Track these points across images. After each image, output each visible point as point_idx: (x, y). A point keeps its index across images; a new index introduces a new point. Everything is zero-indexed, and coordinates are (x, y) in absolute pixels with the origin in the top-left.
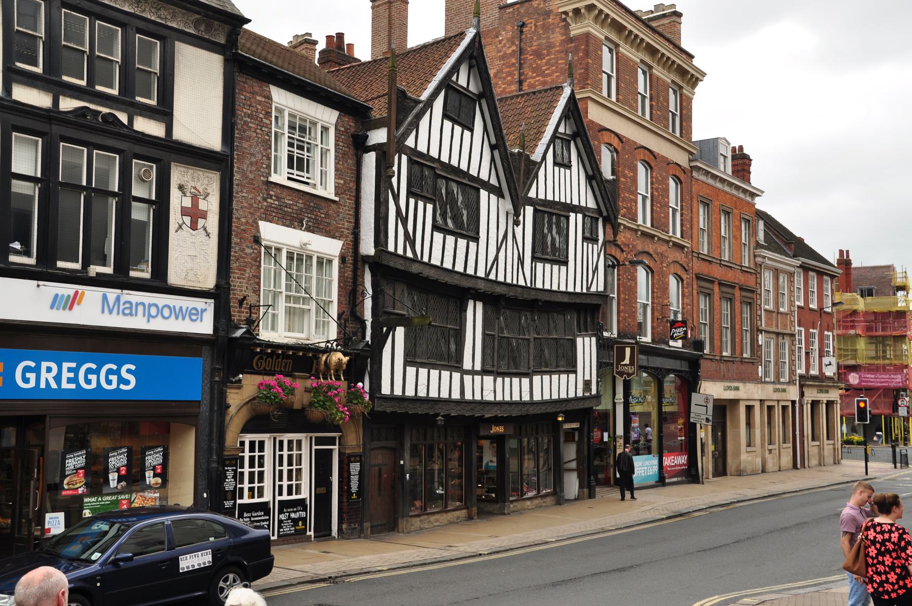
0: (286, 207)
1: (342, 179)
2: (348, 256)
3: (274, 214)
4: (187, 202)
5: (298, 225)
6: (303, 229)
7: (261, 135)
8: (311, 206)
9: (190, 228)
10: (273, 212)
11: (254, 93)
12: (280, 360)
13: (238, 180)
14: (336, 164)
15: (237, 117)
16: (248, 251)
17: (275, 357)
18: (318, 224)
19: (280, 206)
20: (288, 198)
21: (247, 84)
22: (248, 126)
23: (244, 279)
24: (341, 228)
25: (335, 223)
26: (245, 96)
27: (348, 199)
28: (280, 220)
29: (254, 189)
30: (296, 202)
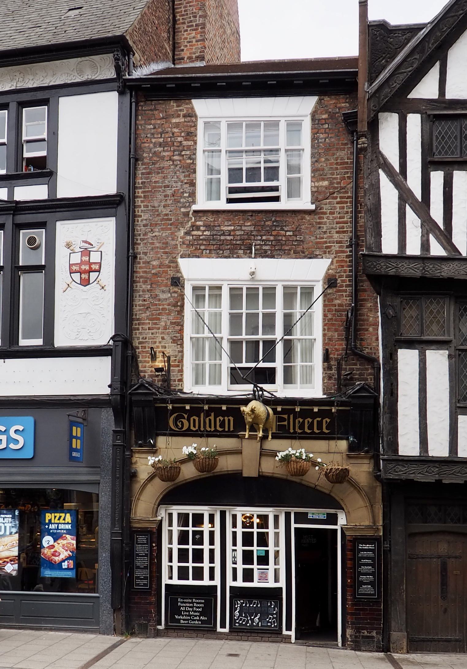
0: (223, 234)
1: (323, 180)
2: (341, 276)
3: (202, 247)
4: (76, 258)
5: (245, 253)
6: (253, 255)
7: (180, 161)
8: (268, 225)
9: (80, 284)
10: (202, 244)
11: (167, 118)
12: (212, 417)
13: (146, 220)
14: (313, 164)
15: (144, 151)
16: (162, 296)
17: (202, 415)
18: (282, 245)
19: (213, 235)
20: (226, 223)
21: (156, 110)
22: (158, 157)
23: (159, 329)
24: (326, 242)
25: (313, 238)
26: (153, 125)
27: (338, 203)
28: (213, 252)
29: (171, 224)
30: (241, 226)
